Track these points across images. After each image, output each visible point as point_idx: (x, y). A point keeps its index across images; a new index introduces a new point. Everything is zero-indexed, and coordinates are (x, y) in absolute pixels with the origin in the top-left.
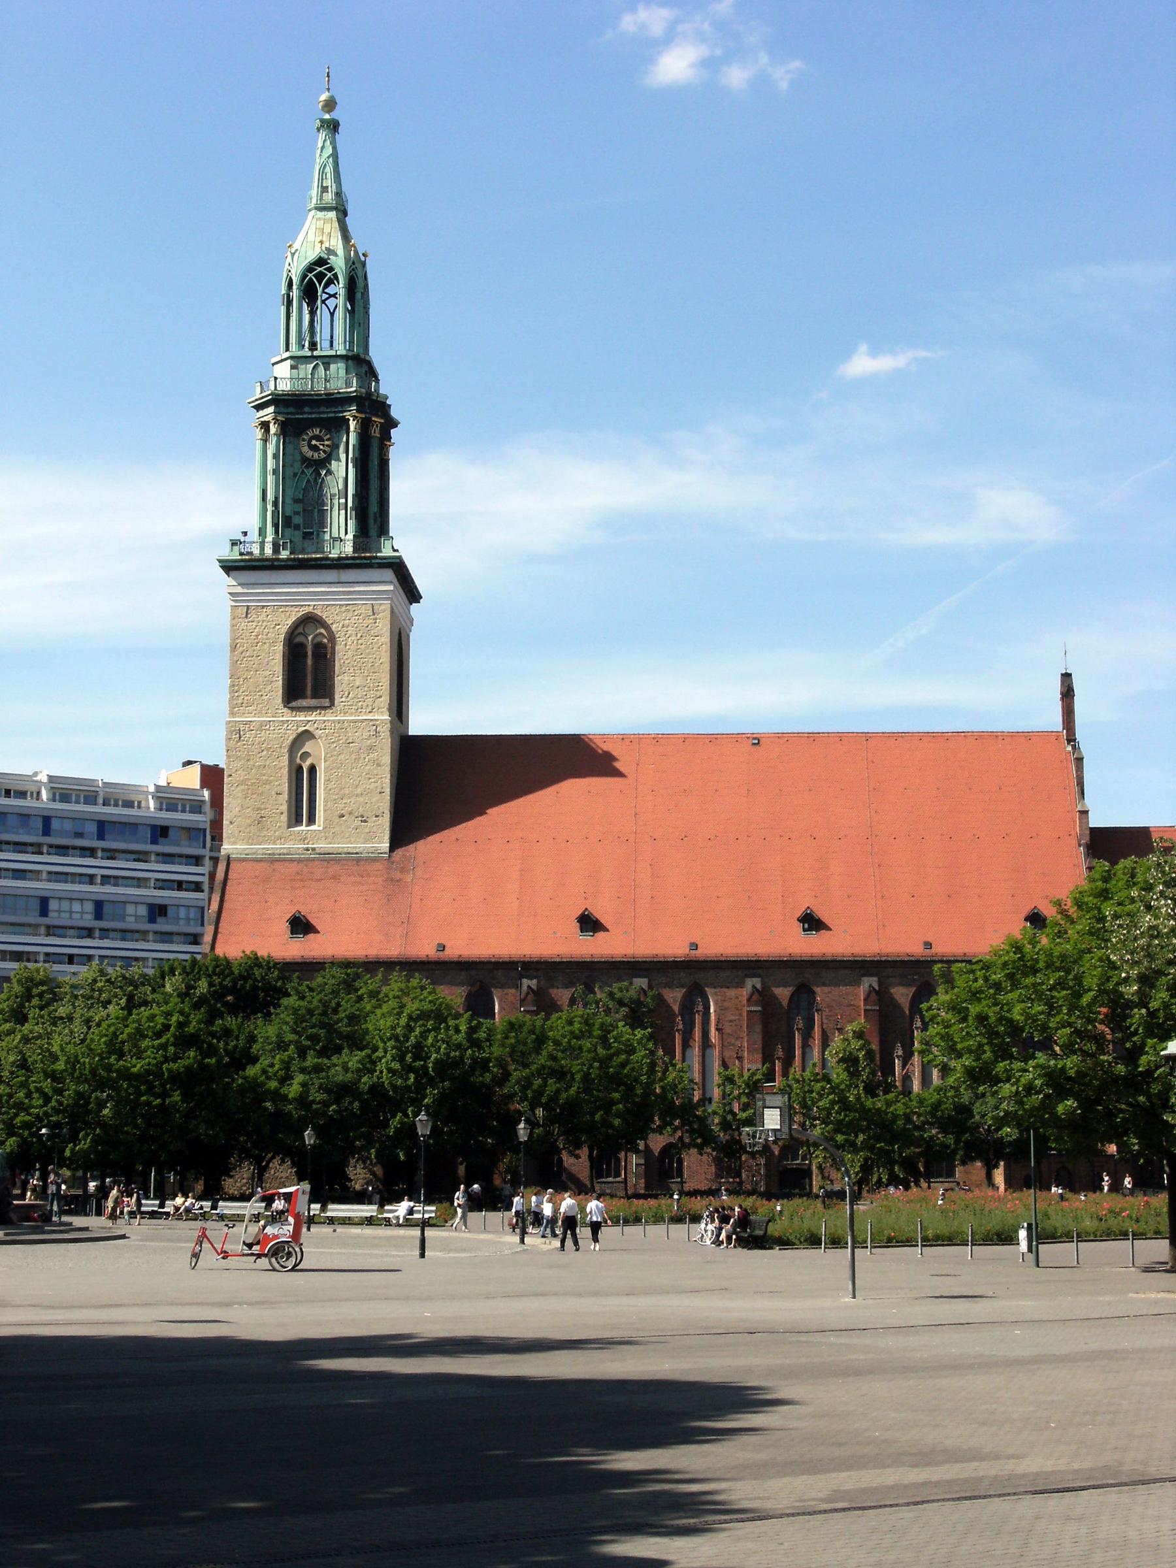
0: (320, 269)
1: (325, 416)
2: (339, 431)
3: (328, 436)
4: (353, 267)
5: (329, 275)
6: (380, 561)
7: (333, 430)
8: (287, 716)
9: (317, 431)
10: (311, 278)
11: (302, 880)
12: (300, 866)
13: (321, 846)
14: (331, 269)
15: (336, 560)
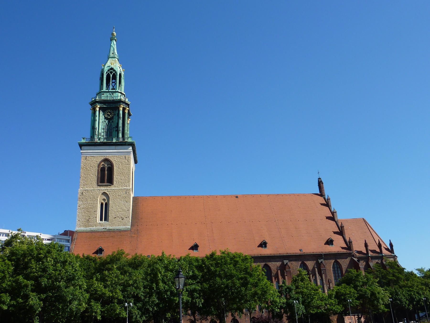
0: (111, 71)
1: (112, 106)
2: (115, 111)
3: (113, 112)
4: (120, 71)
5: (114, 72)
6: (128, 143)
7: (114, 110)
8: (99, 188)
9: (109, 111)
10: (108, 73)
11: (102, 238)
12: (102, 233)
13: (108, 227)
14: (114, 71)
15: (115, 143)
